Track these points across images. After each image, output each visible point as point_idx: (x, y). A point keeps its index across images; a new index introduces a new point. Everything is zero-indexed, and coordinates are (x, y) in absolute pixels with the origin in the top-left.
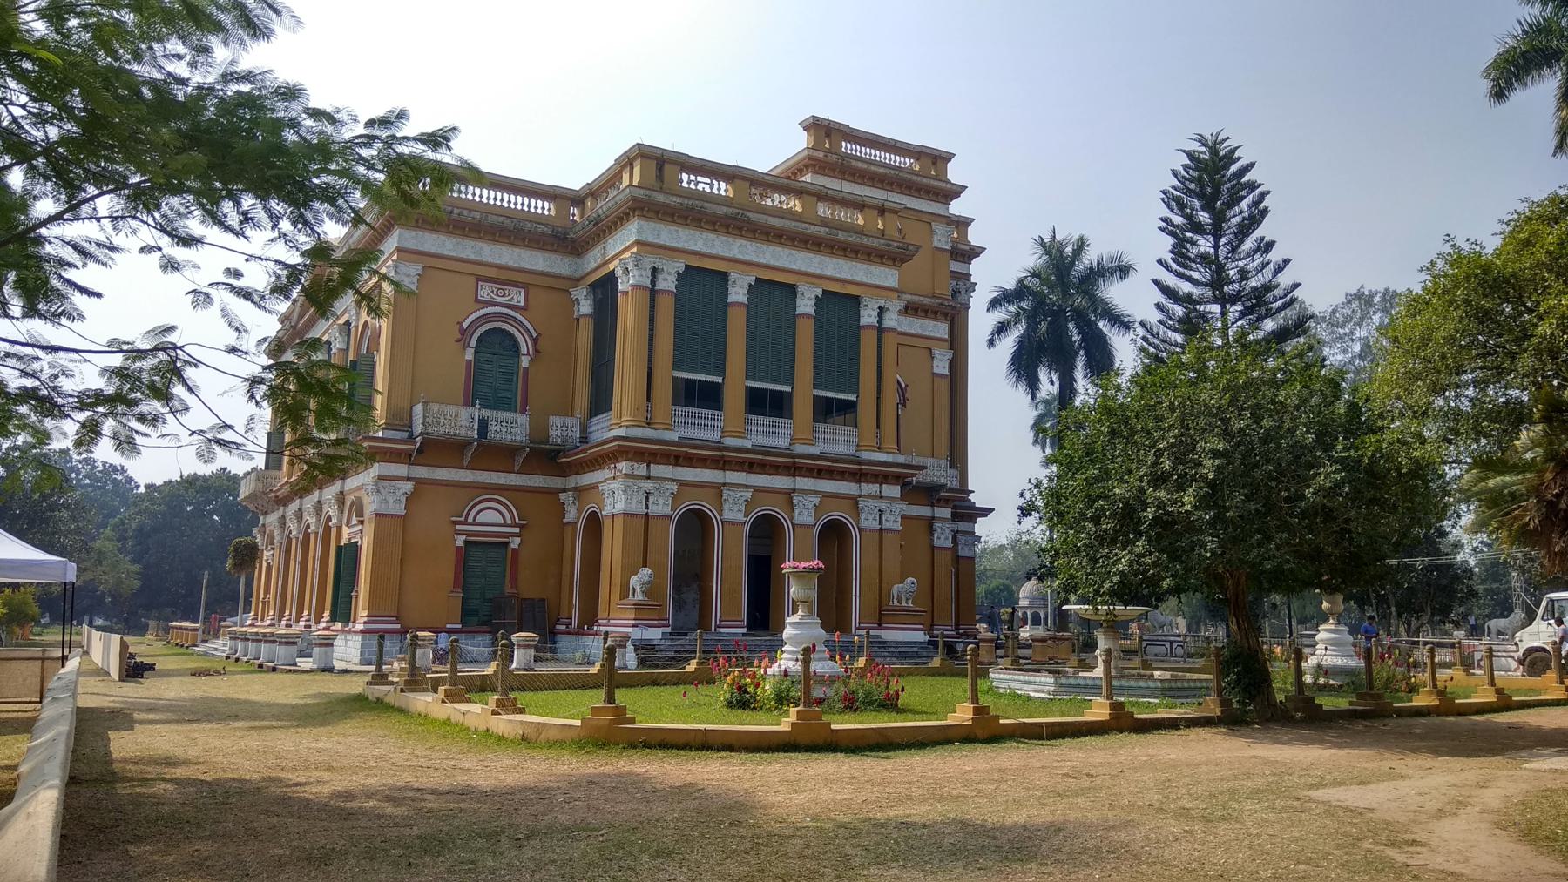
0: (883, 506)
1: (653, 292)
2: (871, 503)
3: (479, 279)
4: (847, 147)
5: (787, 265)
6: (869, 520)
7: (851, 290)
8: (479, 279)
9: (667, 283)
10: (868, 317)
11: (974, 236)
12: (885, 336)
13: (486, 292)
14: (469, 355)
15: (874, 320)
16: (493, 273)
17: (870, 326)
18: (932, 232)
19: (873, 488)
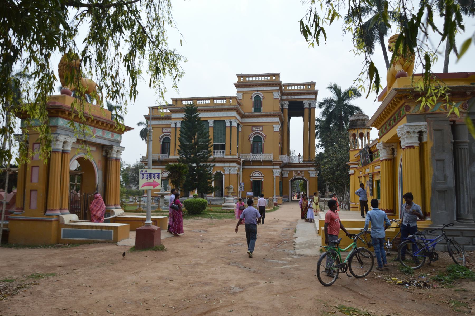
0: (230, 168)
1: (176, 128)
2: (227, 168)
3: (163, 128)
4: (248, 79)
5: (205, 116)
6: (227, 172)
7: (222, 119)
8: (163, 128)
9: (179, 125)
10: (228, 124)
11: (316, 88)
12: (232, 128)
13: (164, 130)
14: (161, 143)
15: (229, 125)
16: (165, 126)
17: (228, 126)
18: (273, 95)
19: (228, 165)
